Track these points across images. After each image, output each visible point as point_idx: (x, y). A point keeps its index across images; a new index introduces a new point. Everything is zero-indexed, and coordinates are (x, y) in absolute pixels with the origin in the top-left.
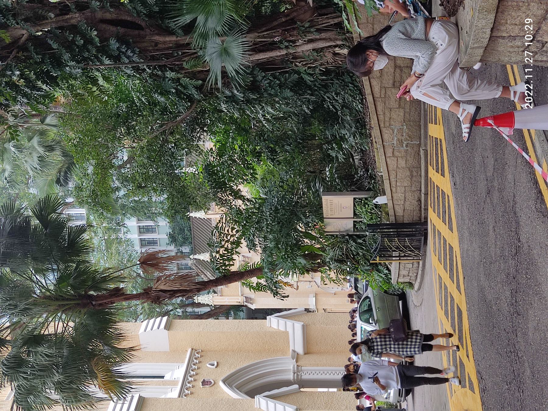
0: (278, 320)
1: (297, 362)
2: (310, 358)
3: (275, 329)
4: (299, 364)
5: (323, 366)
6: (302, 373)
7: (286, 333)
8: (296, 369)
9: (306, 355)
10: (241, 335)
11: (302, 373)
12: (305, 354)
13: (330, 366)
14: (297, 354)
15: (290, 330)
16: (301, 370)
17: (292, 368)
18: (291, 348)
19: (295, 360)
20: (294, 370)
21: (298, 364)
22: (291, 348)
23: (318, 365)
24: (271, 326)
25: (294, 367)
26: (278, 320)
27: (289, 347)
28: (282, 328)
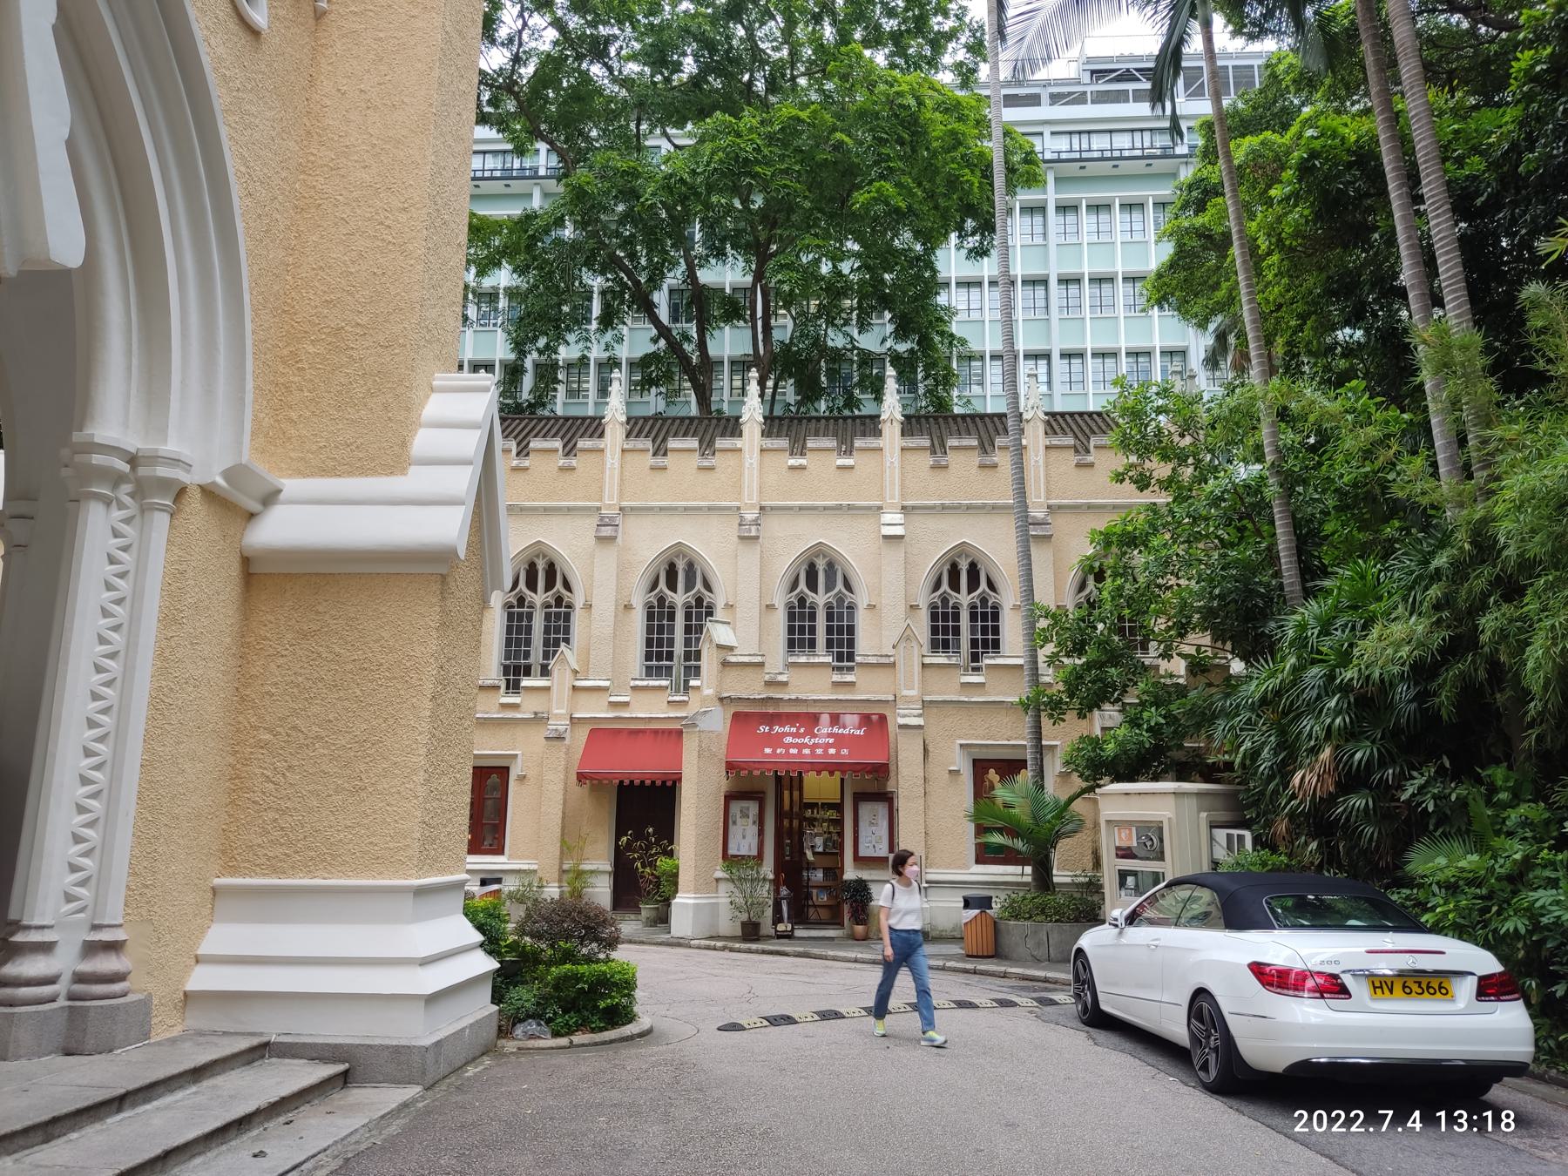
0: (474, 426)
1: (209, 493)
2: (223, 586)
3: (422, 405)
4: (194, 502)
5: (160, 655)
6: (117, 514)
7: (396, 460)
8: (162, 471)
9: (235, 570)
10: (403, 217)
11: (123, 514)
12: (246, 561)
13: (158, 703)
14: (252, 516)
15: (416, 481)
16: (143, 510)
17: (171, 447)
18: (291, 486)
19: (220, 481)
20: (155, 459)
21: (194, 502)
22: (291, 486)
23: (169, 619)
24: (432, 390)
25: (175, 462)
26: (474, 426)
27: (300, 473)
28: (423, 441)
